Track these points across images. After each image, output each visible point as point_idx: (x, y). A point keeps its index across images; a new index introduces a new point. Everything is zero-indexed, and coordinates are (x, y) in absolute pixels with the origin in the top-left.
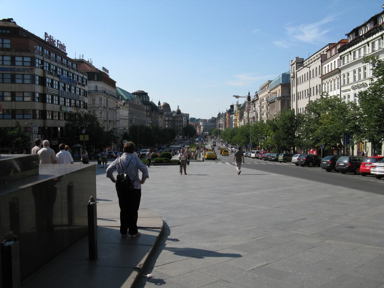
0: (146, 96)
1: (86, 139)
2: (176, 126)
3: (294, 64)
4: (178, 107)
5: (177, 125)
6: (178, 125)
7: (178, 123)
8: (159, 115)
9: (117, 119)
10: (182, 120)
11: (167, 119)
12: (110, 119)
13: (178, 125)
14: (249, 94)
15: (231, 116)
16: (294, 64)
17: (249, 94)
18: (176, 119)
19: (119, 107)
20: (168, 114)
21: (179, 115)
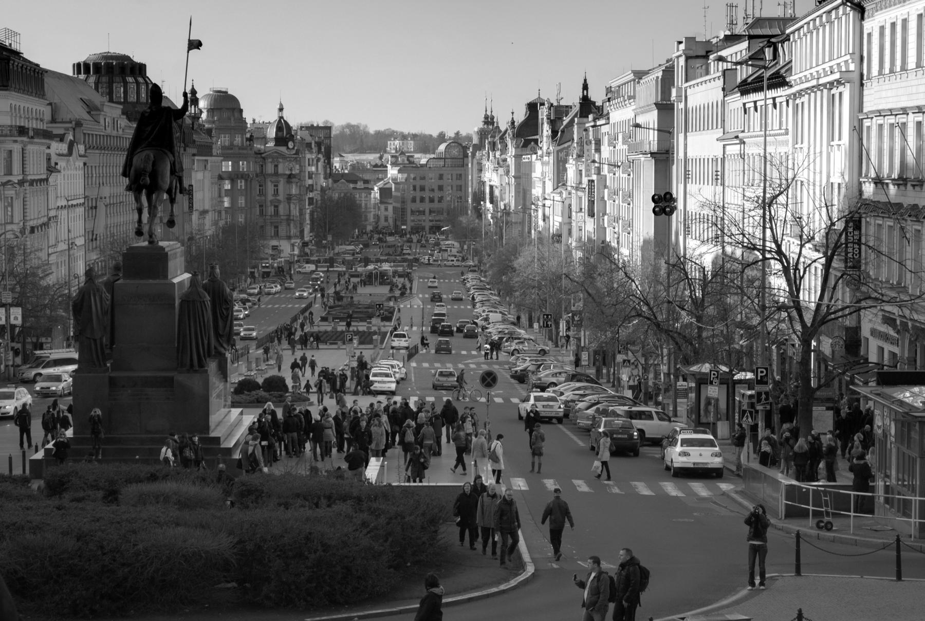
0: (141, 80)
1: (12, 317)
2: (271, 201)
3: (681, 56)
4: (281, 110)
5: (276, 193)
6: (281, 197)
7: (281, 187)
8: (197, 158)
9: (52, 213)
10: (296, 171)
11: (228, 166)
12: (32, 223)
13: (281, 197)
14: (585, 87)
15: (525, 159)
16: (681, 56)
17: (585, 87)
18: (270, 168)
19: (56, 164)
20: (231, 146)
21: (283, 149)
